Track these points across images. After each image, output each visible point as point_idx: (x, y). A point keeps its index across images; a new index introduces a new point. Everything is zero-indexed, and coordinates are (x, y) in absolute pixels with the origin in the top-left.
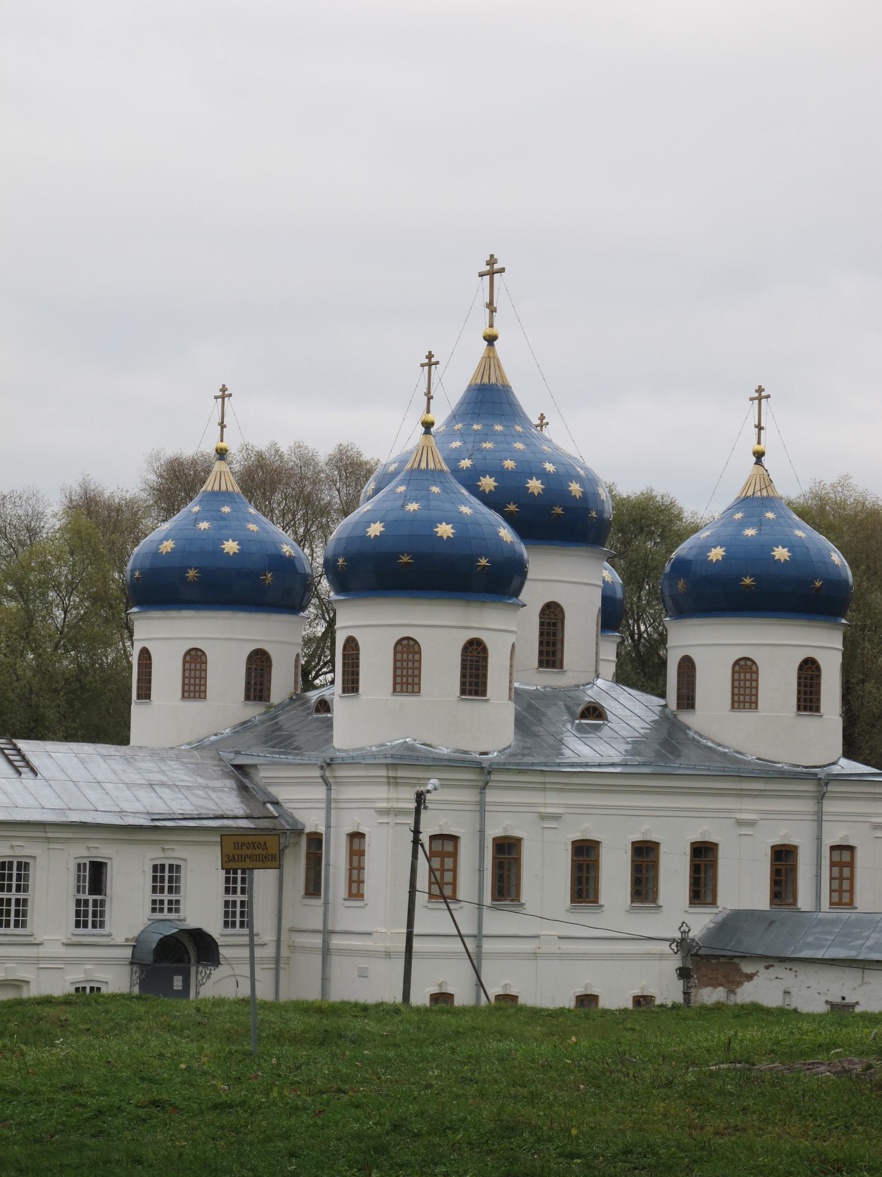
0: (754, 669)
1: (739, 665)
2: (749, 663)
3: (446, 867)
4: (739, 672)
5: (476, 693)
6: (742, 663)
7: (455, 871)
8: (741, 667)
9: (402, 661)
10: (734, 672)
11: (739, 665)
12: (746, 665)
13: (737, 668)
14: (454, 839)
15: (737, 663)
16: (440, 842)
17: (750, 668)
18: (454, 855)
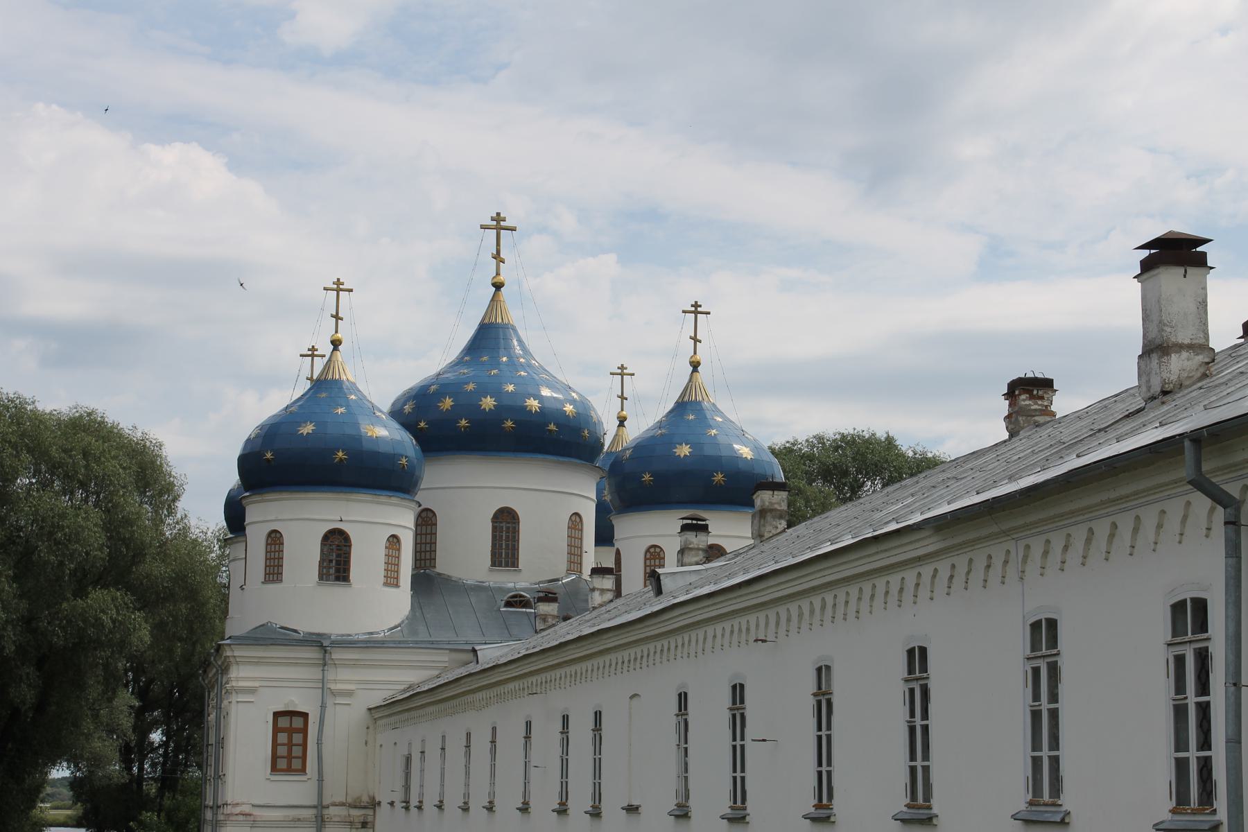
0: (662, 556)
1: (650, 552)
2: (658, 550)
3: (294, 741)
4: (650, 559)
5: (337, 579)
6: (652, 550)
7: (304, 745)
8: (651, 554)
9: (271, 552)
10: (646, 559)
11: (650, 552)
12: (655, 552)
13: (648, 556)
14: (305, 716)
15: (648, 551)
16: (288, 718)
17: (659, 554)
18: (304, 731)
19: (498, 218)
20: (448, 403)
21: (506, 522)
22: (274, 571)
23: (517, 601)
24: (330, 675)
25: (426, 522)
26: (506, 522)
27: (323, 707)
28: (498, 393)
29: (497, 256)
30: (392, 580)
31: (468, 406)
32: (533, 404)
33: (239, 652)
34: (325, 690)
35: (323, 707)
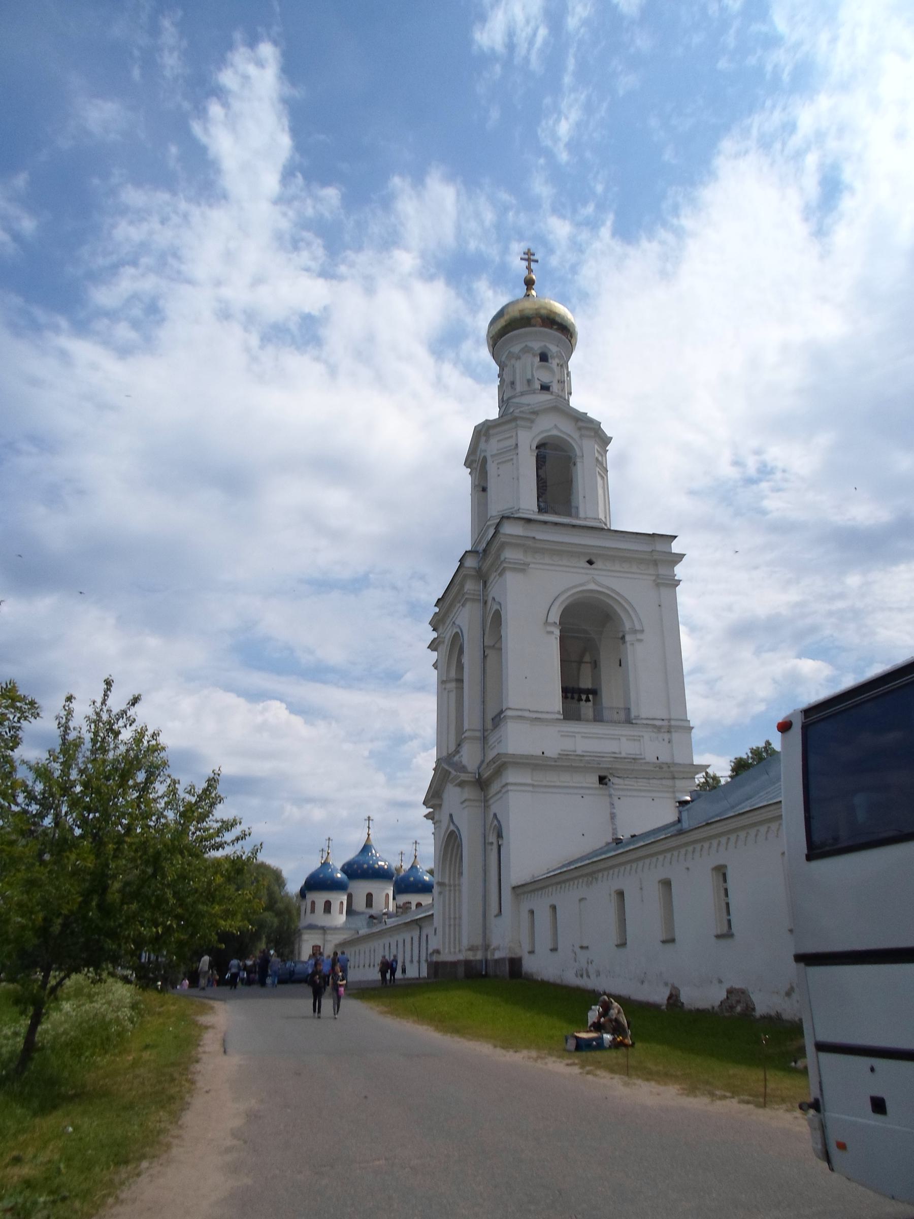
19: (369, 817)
20: (356, 866)
21: (369, 897)
22: (313, 910)
23: (372, 917)
24: (326, 936)
25: (350, 897)
26: (369, 897)
27: (324, 944)
28: (368, 864)
29: (369, 828)
30: (341, 912)
31: (360, 866)
32: (377, 866)
33: (305, 931)
34: (325, 940)
35: (324, 944)
